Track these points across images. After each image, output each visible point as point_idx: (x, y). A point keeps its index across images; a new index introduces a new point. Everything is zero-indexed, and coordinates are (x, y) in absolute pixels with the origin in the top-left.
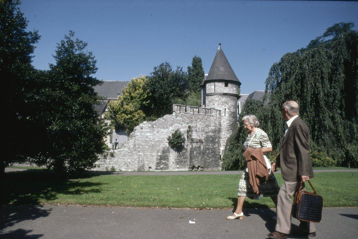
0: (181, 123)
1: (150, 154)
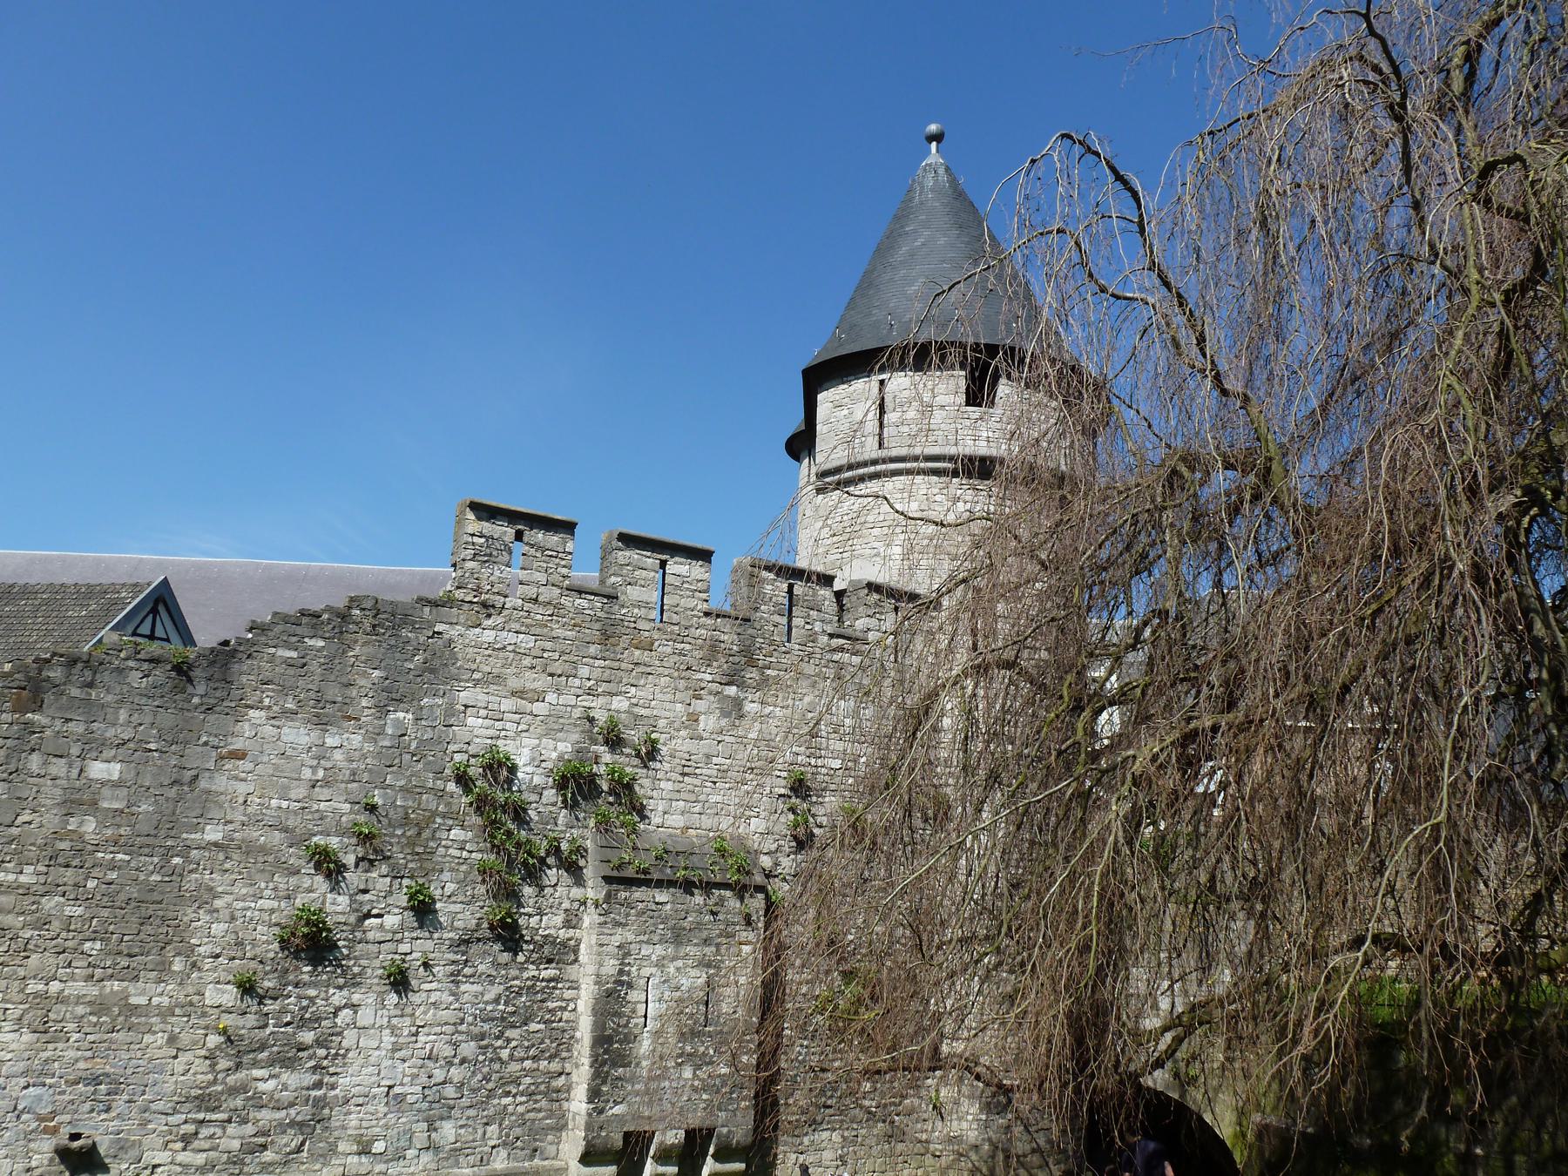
0: (514, 683)
1: (93, 991)
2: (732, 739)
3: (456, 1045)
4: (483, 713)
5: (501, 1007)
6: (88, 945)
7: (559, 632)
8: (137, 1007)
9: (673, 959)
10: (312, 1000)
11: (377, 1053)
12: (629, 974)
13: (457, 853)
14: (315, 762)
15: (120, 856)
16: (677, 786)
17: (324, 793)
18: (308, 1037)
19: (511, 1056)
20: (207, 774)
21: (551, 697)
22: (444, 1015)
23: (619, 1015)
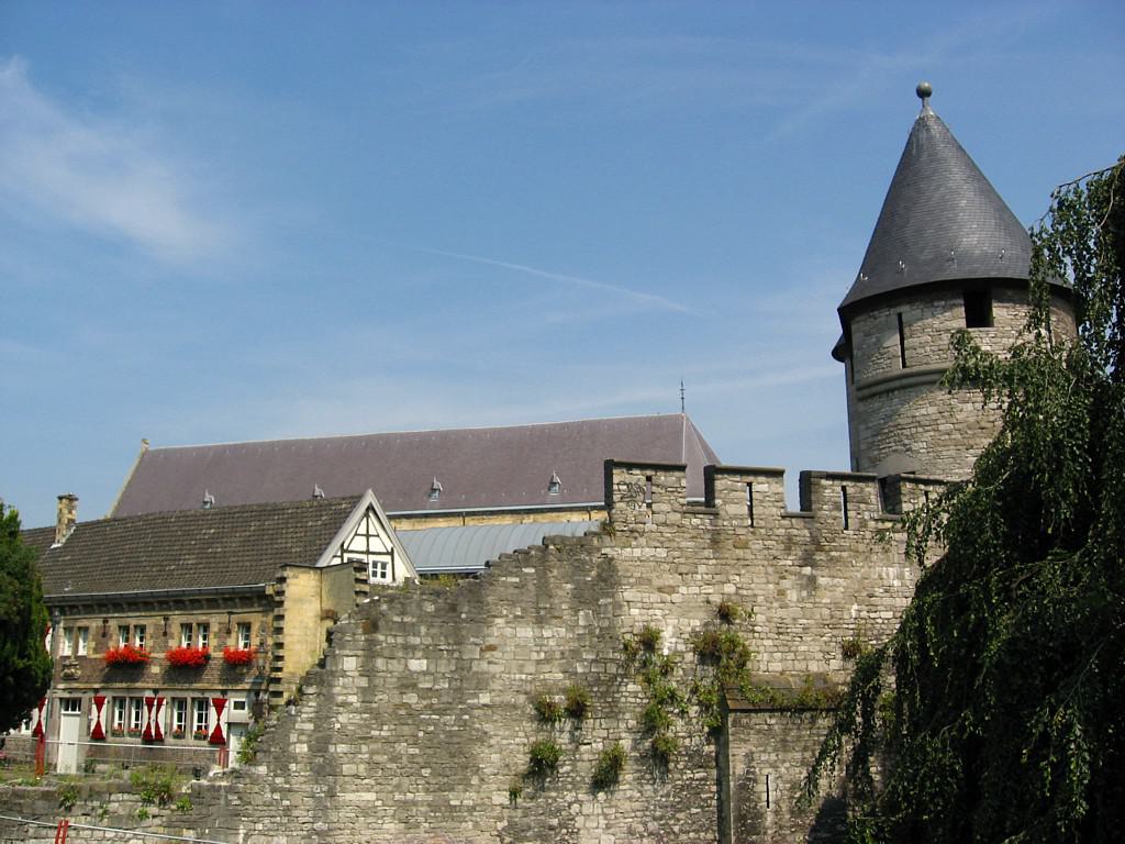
0: (657, 583)
2: (811, 605)
3: (645, 824)
4: (640, 605)
5: (671, 799)
6: (423, 771)
7: (683, 544)
8: (455, 806)
9: (784, 761)
10: (555, 800)
11: (596, 831)
12: (754, 773)
13: (633, 700)
14: (538, 648)
15: (434, 716)
16: (776, 642)
17: (546, 668)
18: (555, 822)
19: (681, 831)
20: (476, 662)
21: (683, 590)
22: (637, 805)
23: (749, 800)
